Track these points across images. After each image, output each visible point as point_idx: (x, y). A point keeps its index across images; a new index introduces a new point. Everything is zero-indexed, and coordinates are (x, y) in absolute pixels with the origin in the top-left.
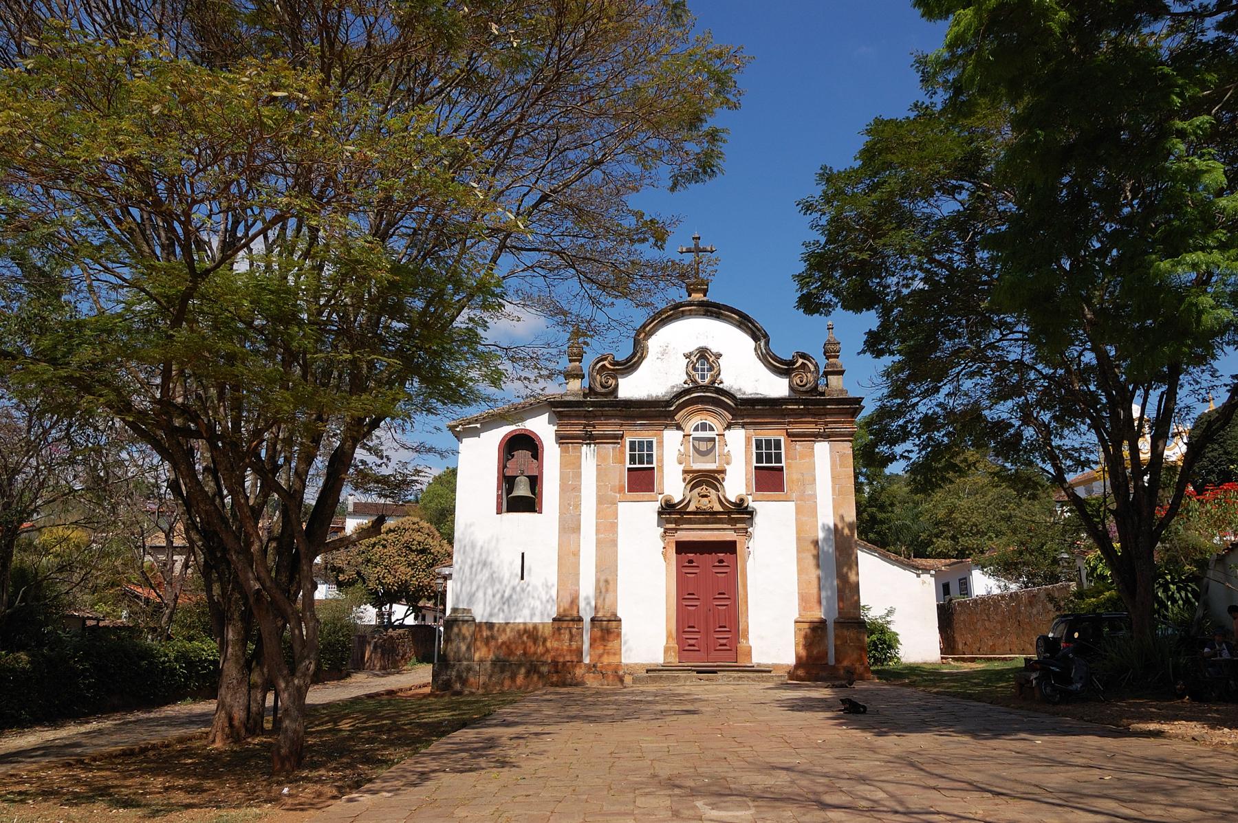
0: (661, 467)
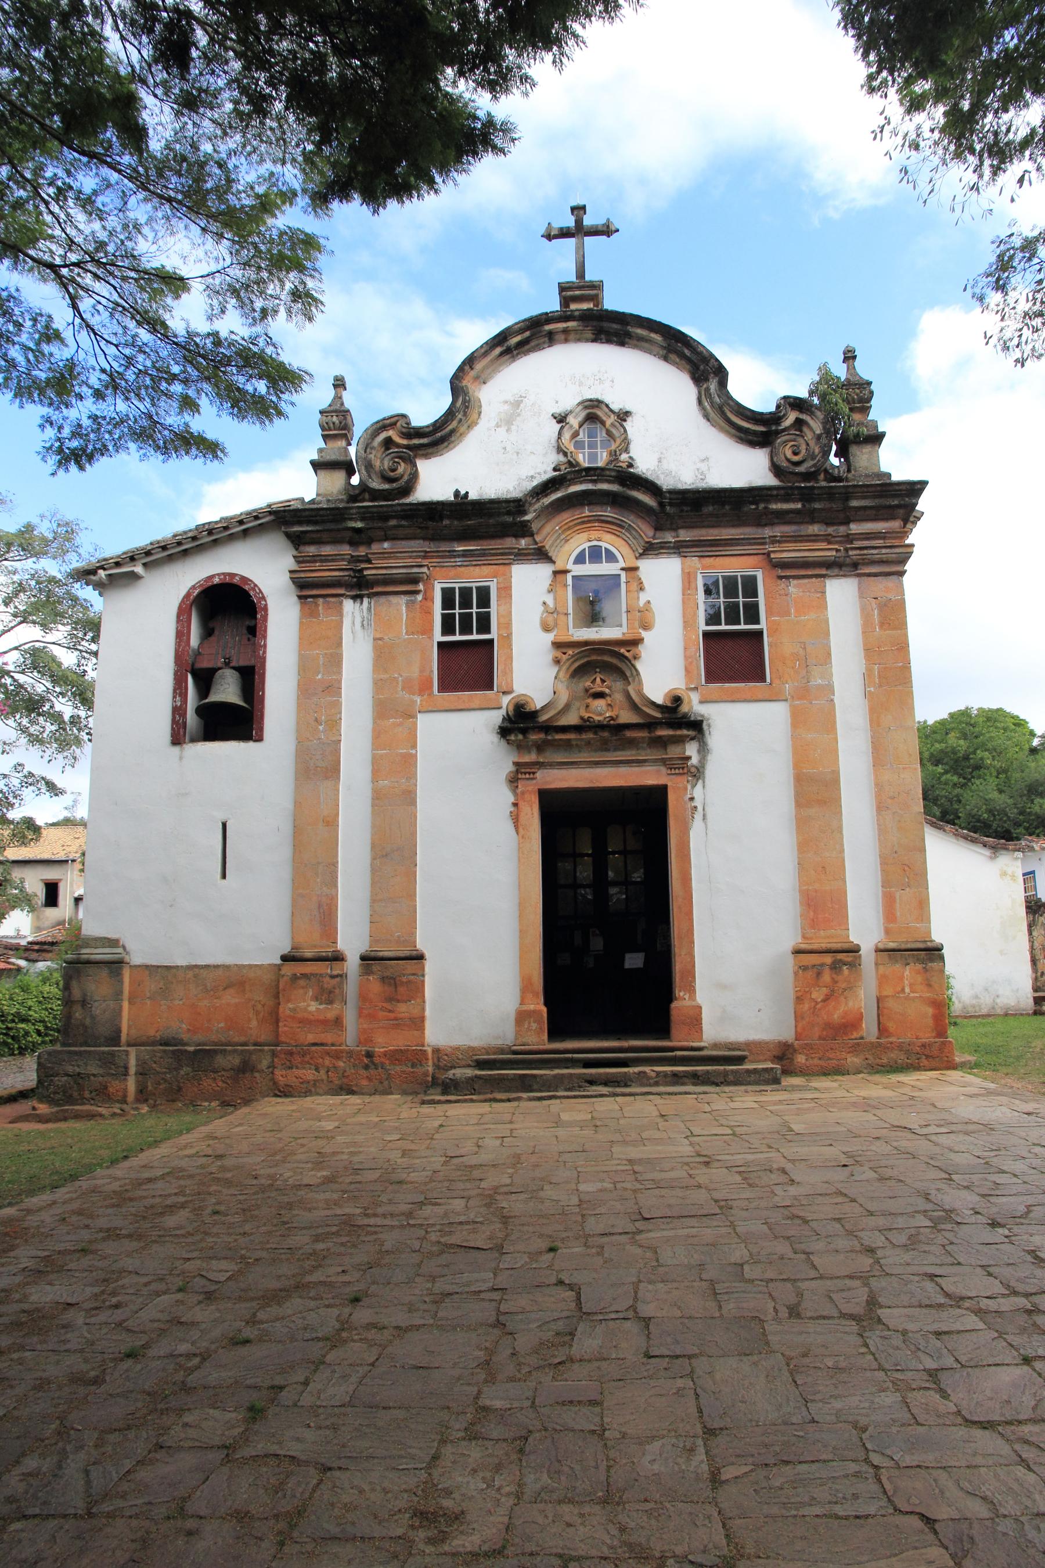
0: (507, 638)
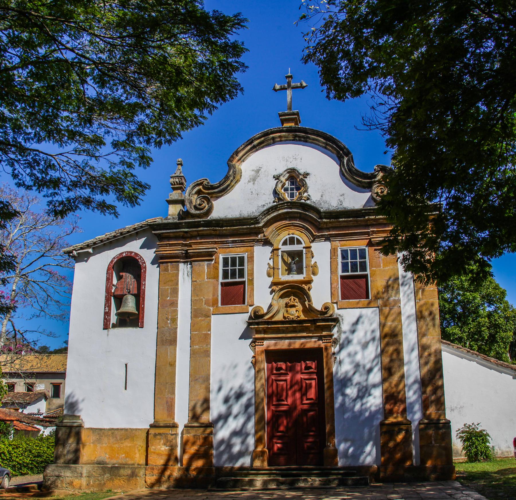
0: (251, 281)
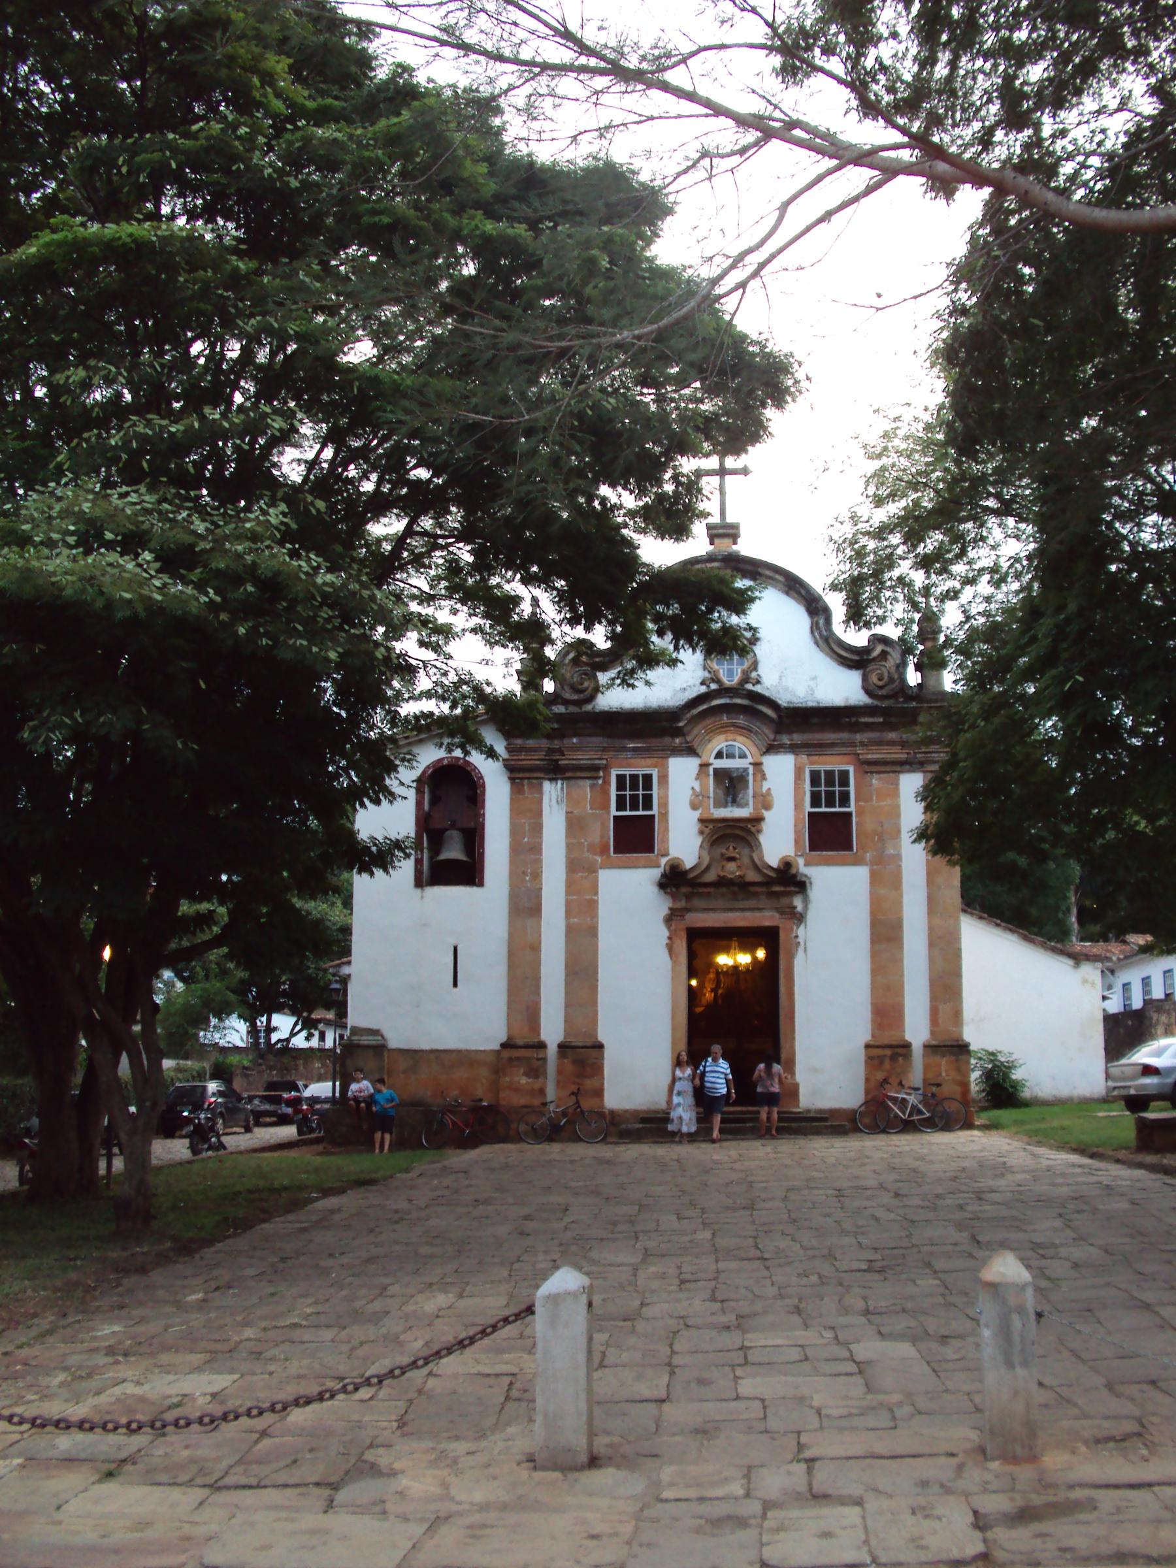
0: (664, 815)
